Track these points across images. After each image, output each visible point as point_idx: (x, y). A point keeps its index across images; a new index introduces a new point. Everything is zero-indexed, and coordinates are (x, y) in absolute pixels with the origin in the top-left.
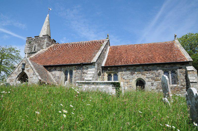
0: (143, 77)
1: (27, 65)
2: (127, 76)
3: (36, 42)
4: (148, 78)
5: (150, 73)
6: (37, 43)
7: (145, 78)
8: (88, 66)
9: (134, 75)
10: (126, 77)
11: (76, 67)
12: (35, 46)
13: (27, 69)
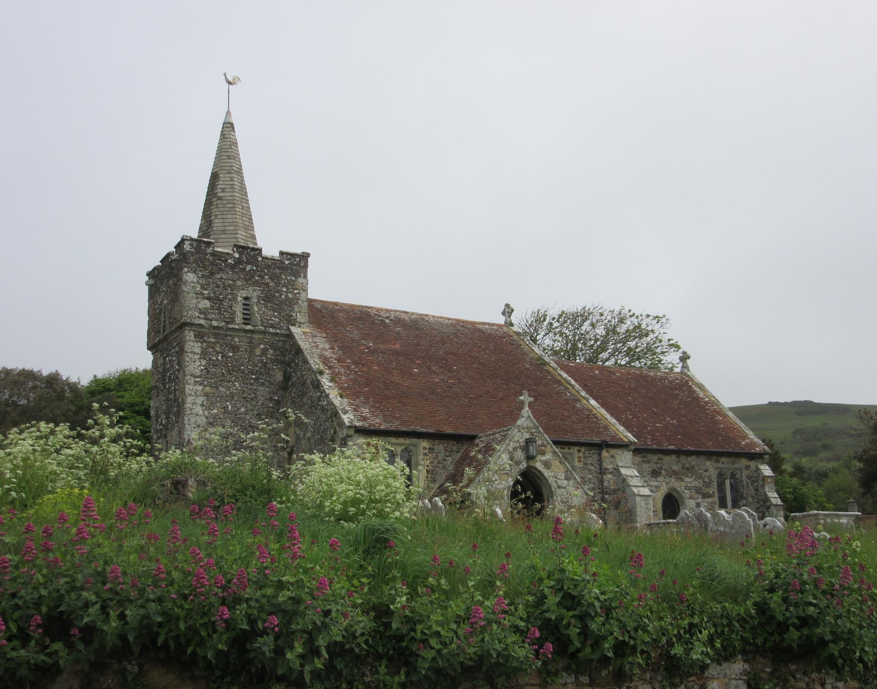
0: (679, 486)
3: (249, 278)
4: (687, 488)
6: (256, 283)
8: (613, 451)
9: (659, 479)
11: (583, 449)
12: (246, 298)
13: (543, 458)
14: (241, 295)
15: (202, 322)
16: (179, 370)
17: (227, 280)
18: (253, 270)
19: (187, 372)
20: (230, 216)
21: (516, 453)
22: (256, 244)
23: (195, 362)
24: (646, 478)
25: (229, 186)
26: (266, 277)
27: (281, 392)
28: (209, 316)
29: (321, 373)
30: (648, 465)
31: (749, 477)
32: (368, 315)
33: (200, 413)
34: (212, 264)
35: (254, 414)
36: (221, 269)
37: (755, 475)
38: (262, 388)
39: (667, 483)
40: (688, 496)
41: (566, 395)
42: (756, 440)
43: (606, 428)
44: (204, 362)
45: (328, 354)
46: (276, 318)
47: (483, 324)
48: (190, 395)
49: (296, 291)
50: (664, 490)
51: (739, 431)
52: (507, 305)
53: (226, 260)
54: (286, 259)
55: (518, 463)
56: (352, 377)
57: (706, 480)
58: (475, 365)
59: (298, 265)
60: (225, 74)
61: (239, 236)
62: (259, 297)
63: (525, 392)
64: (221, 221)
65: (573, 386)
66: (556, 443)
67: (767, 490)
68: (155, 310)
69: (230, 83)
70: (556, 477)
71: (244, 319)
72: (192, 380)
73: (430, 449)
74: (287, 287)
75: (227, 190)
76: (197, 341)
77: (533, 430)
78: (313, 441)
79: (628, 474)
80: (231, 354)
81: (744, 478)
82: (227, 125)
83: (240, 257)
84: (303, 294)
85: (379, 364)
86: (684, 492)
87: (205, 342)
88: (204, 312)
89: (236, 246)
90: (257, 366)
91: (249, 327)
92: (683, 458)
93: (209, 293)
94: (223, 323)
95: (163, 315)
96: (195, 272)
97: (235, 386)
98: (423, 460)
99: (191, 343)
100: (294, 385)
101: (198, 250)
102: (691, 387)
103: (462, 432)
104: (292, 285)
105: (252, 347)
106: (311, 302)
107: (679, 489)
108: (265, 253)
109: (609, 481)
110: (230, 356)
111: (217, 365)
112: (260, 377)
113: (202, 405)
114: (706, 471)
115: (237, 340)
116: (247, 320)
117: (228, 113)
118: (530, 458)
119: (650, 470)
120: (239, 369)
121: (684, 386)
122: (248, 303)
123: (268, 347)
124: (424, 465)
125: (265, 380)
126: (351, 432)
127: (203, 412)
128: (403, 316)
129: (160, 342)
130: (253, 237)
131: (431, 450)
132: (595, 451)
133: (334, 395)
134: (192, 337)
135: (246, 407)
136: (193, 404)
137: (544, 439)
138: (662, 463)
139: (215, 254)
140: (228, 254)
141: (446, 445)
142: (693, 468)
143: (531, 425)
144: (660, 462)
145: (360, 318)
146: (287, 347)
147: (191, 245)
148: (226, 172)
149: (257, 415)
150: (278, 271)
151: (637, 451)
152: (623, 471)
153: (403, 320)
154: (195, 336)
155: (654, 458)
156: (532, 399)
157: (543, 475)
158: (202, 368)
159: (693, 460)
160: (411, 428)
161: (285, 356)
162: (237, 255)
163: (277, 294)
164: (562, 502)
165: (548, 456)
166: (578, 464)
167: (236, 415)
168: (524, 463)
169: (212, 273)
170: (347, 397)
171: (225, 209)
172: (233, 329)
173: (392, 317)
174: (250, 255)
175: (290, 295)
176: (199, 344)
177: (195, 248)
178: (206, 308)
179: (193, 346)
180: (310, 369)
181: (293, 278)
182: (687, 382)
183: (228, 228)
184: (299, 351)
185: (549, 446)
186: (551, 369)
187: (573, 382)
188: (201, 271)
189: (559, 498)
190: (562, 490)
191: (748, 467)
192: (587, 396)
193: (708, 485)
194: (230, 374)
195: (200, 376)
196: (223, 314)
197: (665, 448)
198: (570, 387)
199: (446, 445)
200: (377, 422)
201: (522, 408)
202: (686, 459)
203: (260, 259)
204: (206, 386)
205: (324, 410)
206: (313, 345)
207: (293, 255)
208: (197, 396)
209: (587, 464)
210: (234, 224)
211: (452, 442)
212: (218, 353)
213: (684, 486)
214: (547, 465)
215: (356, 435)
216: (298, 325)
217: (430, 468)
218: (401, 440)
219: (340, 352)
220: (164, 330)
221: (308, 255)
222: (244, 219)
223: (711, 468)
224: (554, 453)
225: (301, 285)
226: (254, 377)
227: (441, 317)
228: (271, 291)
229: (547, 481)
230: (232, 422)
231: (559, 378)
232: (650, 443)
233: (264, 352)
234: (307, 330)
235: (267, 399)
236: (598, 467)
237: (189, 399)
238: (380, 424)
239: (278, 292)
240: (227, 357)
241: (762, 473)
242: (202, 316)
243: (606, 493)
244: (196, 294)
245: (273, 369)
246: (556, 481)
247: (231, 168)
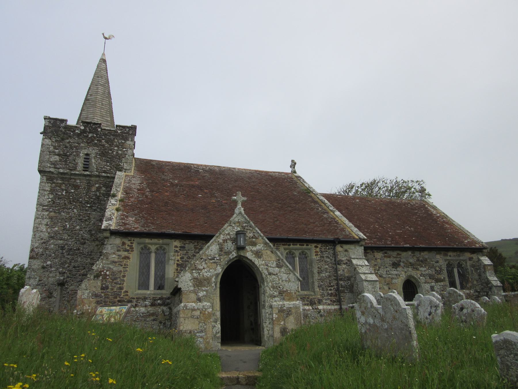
1: (253, 238)
2: (386, 269)
3: (90, 142)
4: (424, 275)
5: (425, 267)
6: (96, 145)
7: (419, 275)
8: (346, 247)
9: (398, 269)
10: (385, 273)
11: (319, 246)
12: (87, 155)
13: (254, 249)
15: (52, 170)
17: (73, 143)
18: (94, 137)
20: (92, 109)
21: (226, 244)
23: (44, 196)
24: (388, 269)
25: (95, 93)
28: (58, 166)
30: (388, 259)
31: (473, 266)
33: (44, 230)
34: (64, 133)
35: (86, 231)
36: (70, 137)
37: (477, 264)
38: (94, 213)
39: (406, 272)
40: (423, 281)
41: (318, 209)
43: (343, 230)
44: (51, 196)
46: (108, 166)
47: (274, 172)
49: (125, 149)
50: (403, 277)
51: (462, 234)
52: (293, 161)
53: (74, 131)
54: (119, 130)
55: (228, 253)
59: (128, 133)
60: (103, 34)
65: (325, 204)
67: (488, 275)
69: (106, 38)
70: (267, 265)
71: (84, 167)
73: (180, 247)
74: (118, 147)
75: (93, 95)
76: (48, 183)
77: (244, 225)
79: (359, 264)
80: (73, 191)
81: (469, 267)
82: (102, 60)
84: (130, 151)
86: (419, 278)
87: (54, 183)
88: (54, 164)
90: (92, 198)
91: (88, 173)
92: (417, 254)
93: (59, 152)
94: (68, 171)
96: (50, 139)
97: (74, 211)
98: (174, 256)
102: (427, 208)
104: (122, 146)
105: (89, 185)
107: (416, 276)
109: (343, 270)
110: (72, 192)
111: (61, 198)
112: (93, 205)
113: (47, 225)
114: (437, 262)
116: (86, 167)
117: (104, 54)
119: (391, 263)
120: (78, 201)
121: (422, 208)
122: (88, 157)
123: (102, 186)
124: (174, 260)
125: (97, 207)
127: (47, 230)
131: (182, 248)
132: (330, 247)
135: (81, 225)
136: (39, 224)
138: (400, 257)
141: (196, 244)
142: (426, 260)
143: (243, 220)
144: (399, 256)
148: (95, 85)
149: (89, 231)
152: (355, 262)
154: (47, 180)
155: (394, 254)
156: (245, 199)
157: (254, 263)
158: (50, 200)
159: (425, 255)
162: (82, 128)
163: (110, 152)
164: (273, 287)
165: (259, 247)
166: (315, 257)
167: (72, 231)
168: (233, 253)
169: (63, 139)
171: (90, 106)
174: (92, 127)
175: (120, 152)
176: (49, 185)
177: (52, 124)
178: (56, 161)
181: (123, 141)
182: (424, 205)
183: (89, 116)
185: (260, 238)
186: (313, 195)
188: (55, 138)
189: (270, 284)
190: (273, 276)
191: (471, 259)
193: (439, 272)
194: (71, 204)
196: (68, 165)
197: (401, 246)
198: (323, 205)
199: (196, 244)
202: (420, 254)
203: (99, 130)
204: (51, 212)
208: (43, 219)
209: (323, 257)
210: (94, 113)
211: (201, 242)
212: (63, 190)
214: (258, 254)
216: (124, 170)
218: (155, 241)
222: (103, 111)
224: (266, 243)
225: (129, 145)
226: (89, 205)
227: (244, 169)
228: (106, 149)
229: (258, 269)
230: (69, 236)
231: (317, 200)
233: (98, 189)
235: (97, 220)
236: (333, 259)
239: (111, 150)
240: (70, 193)
241: (483, 263)
243: (341, 280)
244: (50, 152)
245: (104, 200)
246: (267, 269)
247: (98, 83)
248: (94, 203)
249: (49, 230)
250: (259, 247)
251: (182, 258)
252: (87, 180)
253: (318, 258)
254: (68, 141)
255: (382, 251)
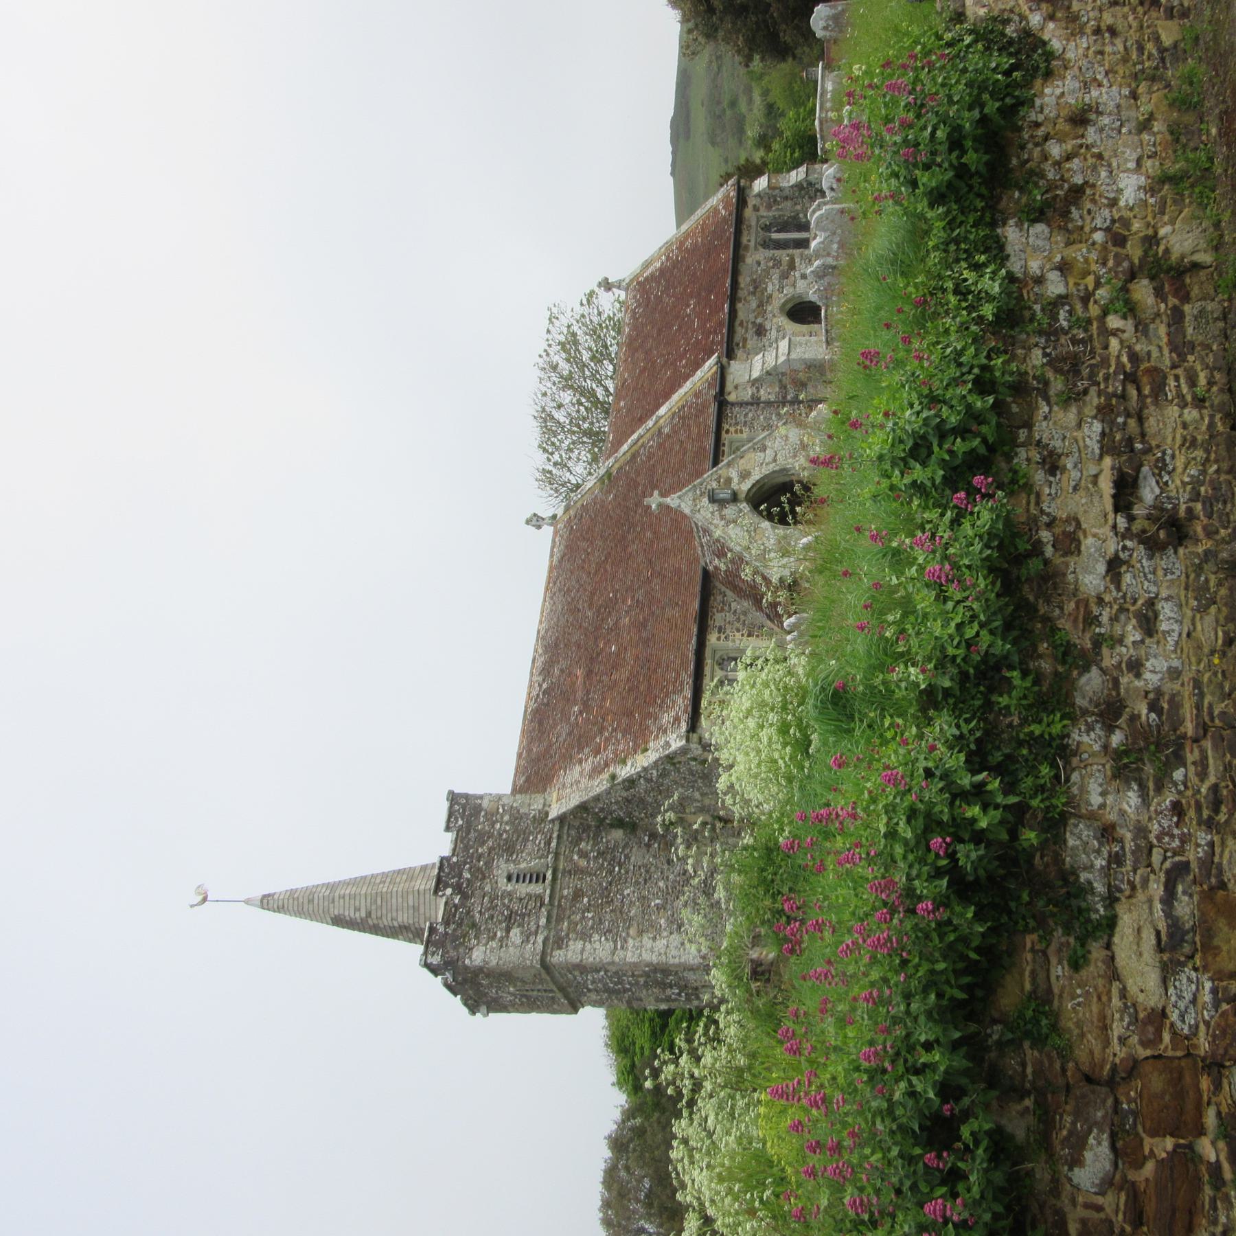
0: (778, 301)
3: (481, 875)
4: (781, 290)
6: (489, 864)
8: (729, 386)
9: (768, 327)
11: (726, 426)
12: (509, 878)
13: (736, 480)
14: (503, 885)
15: (540, 938)
16: (606, 971)
18: (470, 869)
19: (609, 960)
20: (394, 900)
22: (434, 864)
26: (480, 850)
27: (639, 832)
28: (533, 929)
29: (613, 777)
30: (749, 341)
32: (536, 712)
33: (664, 942)
34: (460, 925)
36: (468, 913)
38: (633, 859)
39: (774, 316)
40: (791, 290)
41: (652, 447)
42: (720, 194)
43: (698, 395)
44: (596, 937)
45: (588, 767)
47: (552, 556)
48: (640, 955)
50: (783, 321)
51: (708, 218)
53: (455, 906)
56: (620, 735)
57: (771, 264)
58: (609, 568)
61: (422, 887)
62: (507, 861)
63: (646, 501)
64: (400, 913)
65: (641, 437)
66: (716, 462)
68: (522, 1004)
71: (537, 881)
72: (620, 953)
73: (719, 632)
78: (706, 790)
80: (586, 900)
83: (452, 886)
84: (505, 801)
85: (604, 699)
87: (567, 935)
89: (436, 892)
92: (741, 294)
95: (530, 993)
96: (471, 949)
98: (734, 641)
99: (570, 954)
100: (630, 815)
101: (440, 944)
102: (646, 279)
103: (698, 588)
106: (516, 790)
108: (447, 852)
114: (759, 263)
115: (565, 892)
116: (539, 878)
118: (735, 498)
126: (694, 737)
128: (538, 664)
129: (566, 997)
130: (424, 868)
133: (643, 761)
134: (562, 952)
137: (710, 479)
139: (446, 922)
140: (446, 903)
142: (754, 281)
143: (690, 494)
145: (540, 723)
146: (577, 823)
147: (433, 954)
150: (472, 835)
151: (730, 354)
152: (756, 374)
153: (544, 664)
154: (560, 948)
155: (740, 331)
156: (656, 493)
157: (758, 482)
159: (744, 281)
160: (691, 656)
161: (589, 827)
162: (449, 891)
163: (505, 836)
164: (795, 456)
165: (733, 474)
169: (473, 925)
170: (647, 742)
172: (551, 897)
173: (540, 679)
175: (506, 818)
176: (571, 943)
178: (522, 933)
179: (573, 952)
180: (608, 792)
182: (639, 283)
184: (583, 807)
186: (617, 466)
187: (635, 436)
192: (654, 418)
193: (777, 263)
195: (615, 942)
200: (682, 701)
201: (668, 507)
203: (455, 859)
204: (628, 934)
205: (663, 775)
206: (575, 787)
207: (451, 814)
212: (583, 917)
213: (779, 294)
214: (744, 475)
215: (699, 731)
217: (745, 632)
219: (586, 751)
220: (551, 991)
221: (451, 793)
223: (755, 258)
224: (729, 465)
229: (766, 476)
231: (628, 455)
232: (720, 337)
233: (583, 855)
234: (555, 795)
237: (646, 957)
238: (685, 697)
242: (532, 939)
243: (784, 397)
245: (607, 842)
248: (613, 859)
249: (665, 934)
250: (733, 474)
251: (738, 631)
252: (563, 874)
253: (746, 430)
254: (477, 916)
255: (733, 350)
